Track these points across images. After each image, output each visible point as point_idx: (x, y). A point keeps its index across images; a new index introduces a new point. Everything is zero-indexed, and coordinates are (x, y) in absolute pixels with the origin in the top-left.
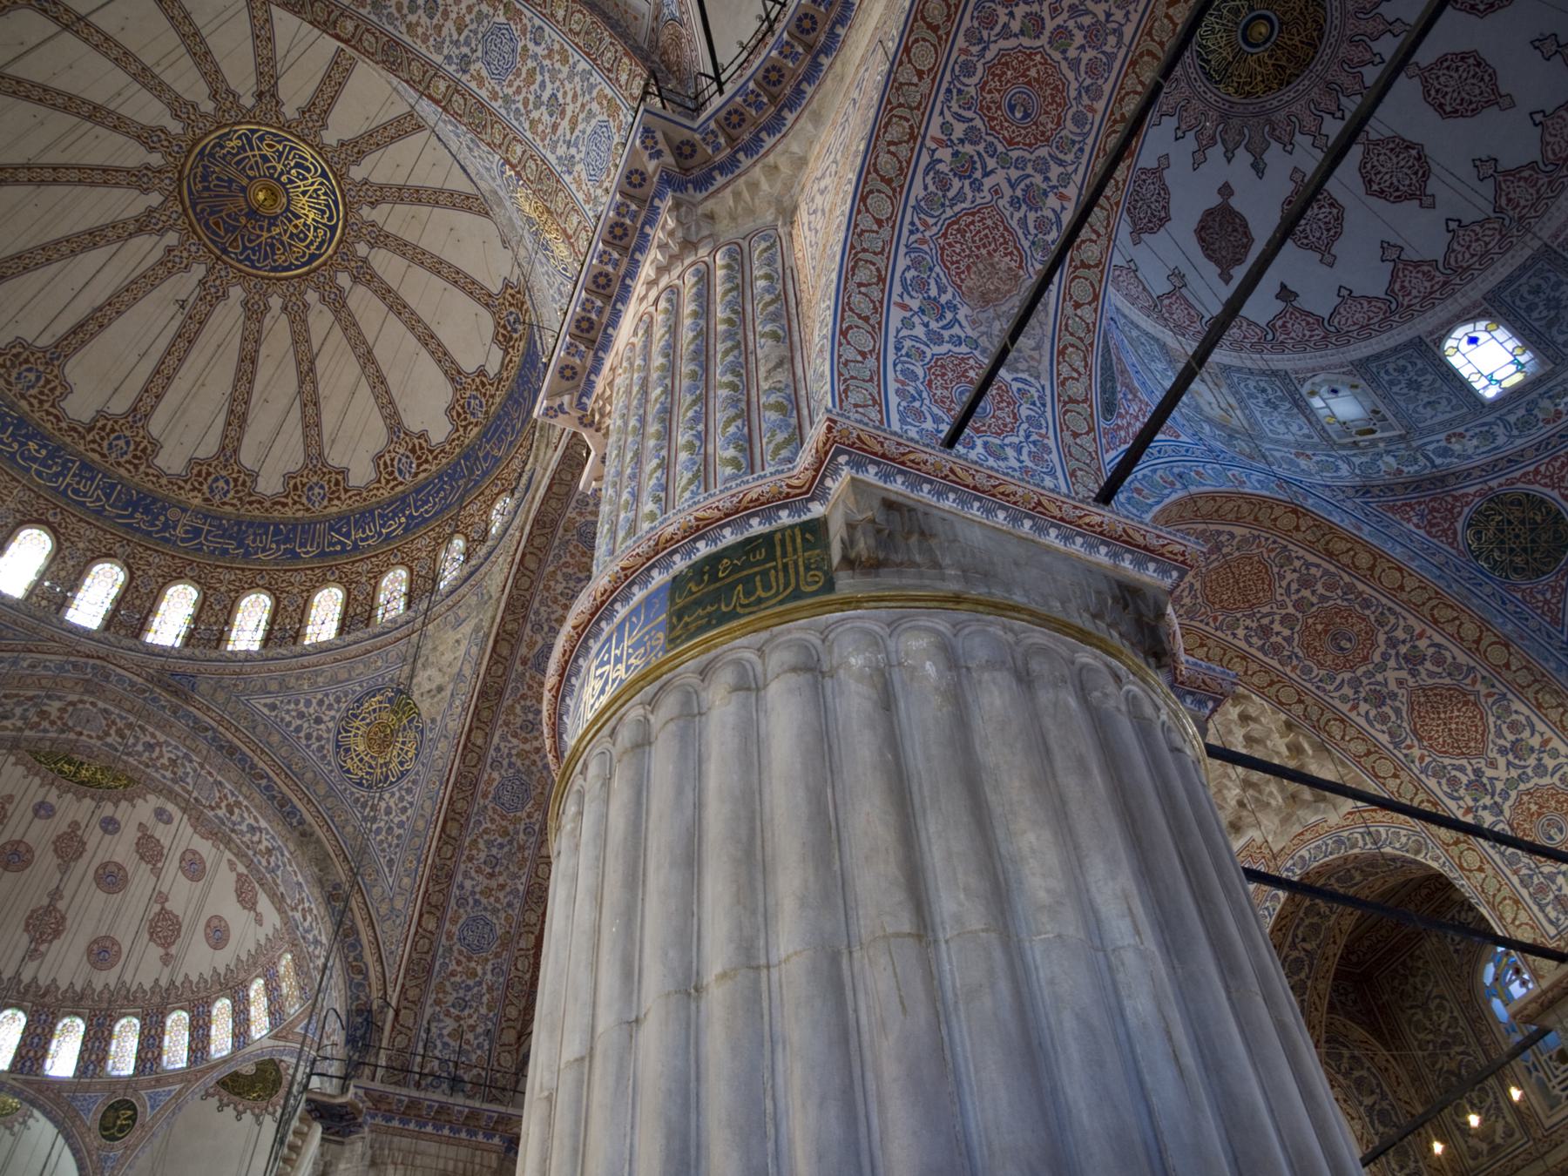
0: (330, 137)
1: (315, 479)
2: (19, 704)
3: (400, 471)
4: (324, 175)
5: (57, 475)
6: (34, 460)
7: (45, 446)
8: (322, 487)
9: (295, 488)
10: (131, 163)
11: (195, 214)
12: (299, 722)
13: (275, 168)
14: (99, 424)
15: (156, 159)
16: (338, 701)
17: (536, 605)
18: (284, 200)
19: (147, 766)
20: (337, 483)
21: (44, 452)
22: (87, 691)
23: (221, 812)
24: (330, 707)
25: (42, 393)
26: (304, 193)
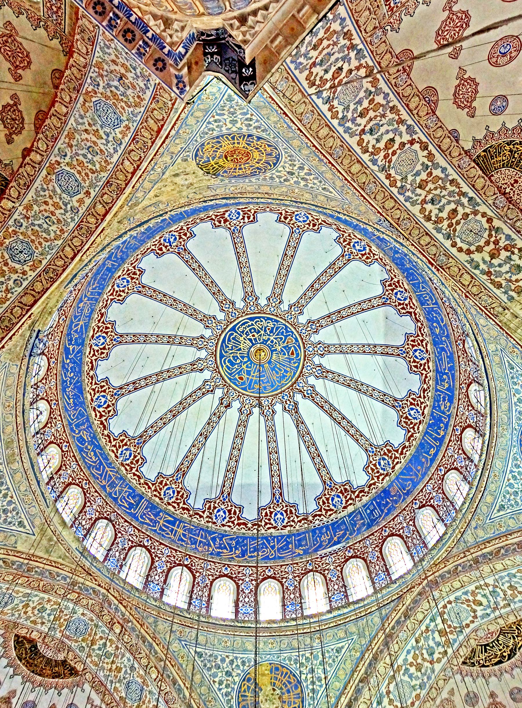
0: (207, 374)
1: (299, 224)
2: (499, 274)
3: (239, 214)
4: (222, 356)
5: (435, 311)
6: (440, 326)
7: (432, 324)
8: (296, 219)
9: (314, 225)
10: (308, 403)
11: (299, 364)
12: (307, 177)
13: (247, 367)
14: (404, 311)
15: (298, 397)
16: (272, 178)
17: (72, 225)
18: (252, 349)
19: (452, 182)
20: (286, 218)
21: (435, 324)
22: (448, 256)
23: (406, 138)
24: (279, 177)
25: (419, 344)
26: (240, 349)
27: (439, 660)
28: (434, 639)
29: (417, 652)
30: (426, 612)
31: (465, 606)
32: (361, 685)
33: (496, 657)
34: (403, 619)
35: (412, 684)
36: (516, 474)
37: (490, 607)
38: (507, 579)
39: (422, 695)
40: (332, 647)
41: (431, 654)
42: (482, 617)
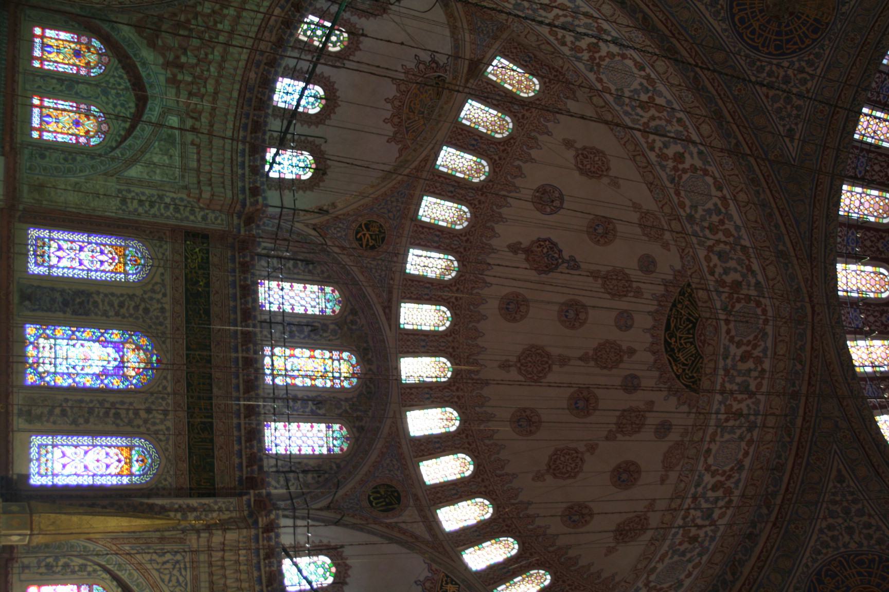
27: (708, 259)
28: (735, 270)
29: (731, 239)
30: (771, 283)
31: (751, 338)
32: (734, 141)
33: (675, 326)
34: (781, 247)
35: (700, 209)
36: (871, 531)
37: (734, 367)
38: (752, 418)
39: (681, 211)
40: (800, 126)
41: (720, 255)
42: (726, 349)
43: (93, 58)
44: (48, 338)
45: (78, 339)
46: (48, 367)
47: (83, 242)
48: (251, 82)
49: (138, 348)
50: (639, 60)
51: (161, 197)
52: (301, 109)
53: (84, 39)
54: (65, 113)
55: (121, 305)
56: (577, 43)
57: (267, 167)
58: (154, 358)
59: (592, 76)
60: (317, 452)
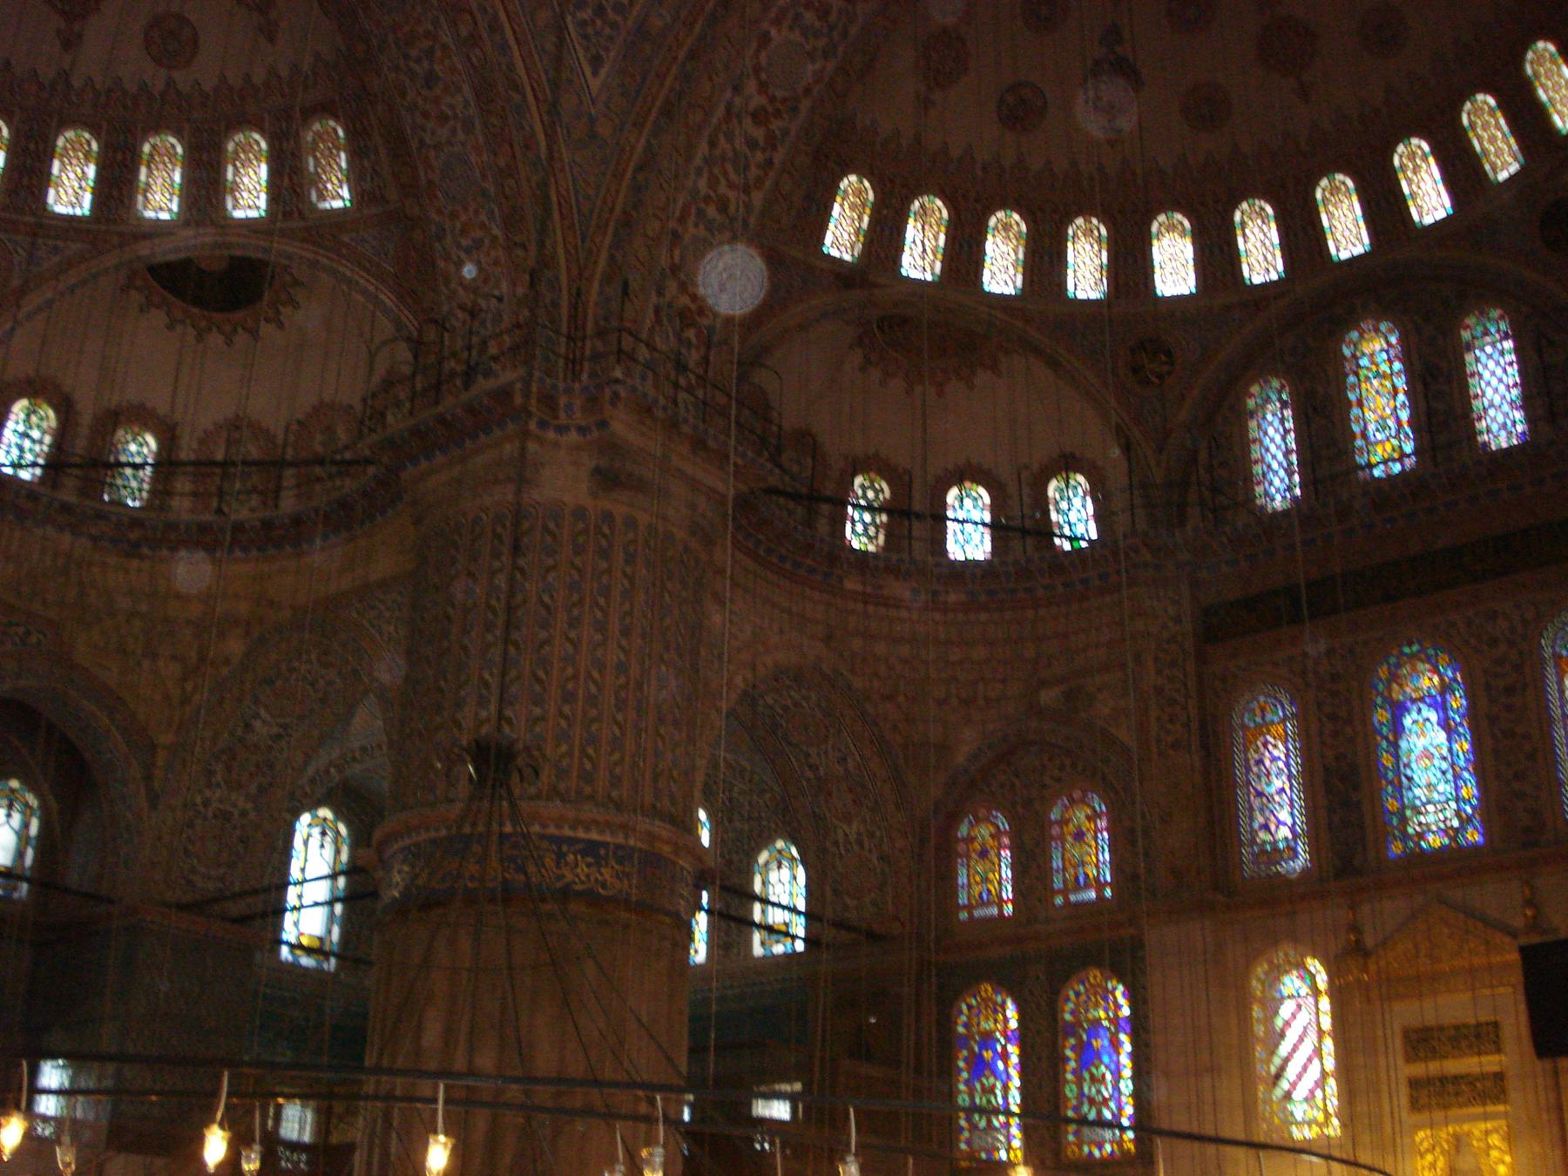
43: (984, 831)
44: (1404, 821)
45: (1398, 773)
46: (1448, 814)
47: (1249, 794)
48: (963, 597)
49: (1394, 677)
50: (754, 45)
51: (1159, 691)
52: (987, 518)
53: (961, 848)
54: (1068, 855)
55: (1333, 717)
56: (761, 142)
57: (1084, 544)
58: (1406, 650)
59: (805, 105)
60: (1513, 357)
